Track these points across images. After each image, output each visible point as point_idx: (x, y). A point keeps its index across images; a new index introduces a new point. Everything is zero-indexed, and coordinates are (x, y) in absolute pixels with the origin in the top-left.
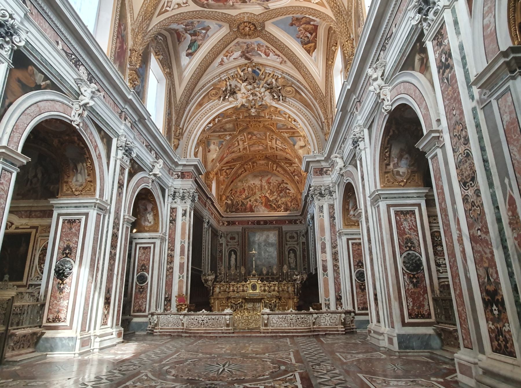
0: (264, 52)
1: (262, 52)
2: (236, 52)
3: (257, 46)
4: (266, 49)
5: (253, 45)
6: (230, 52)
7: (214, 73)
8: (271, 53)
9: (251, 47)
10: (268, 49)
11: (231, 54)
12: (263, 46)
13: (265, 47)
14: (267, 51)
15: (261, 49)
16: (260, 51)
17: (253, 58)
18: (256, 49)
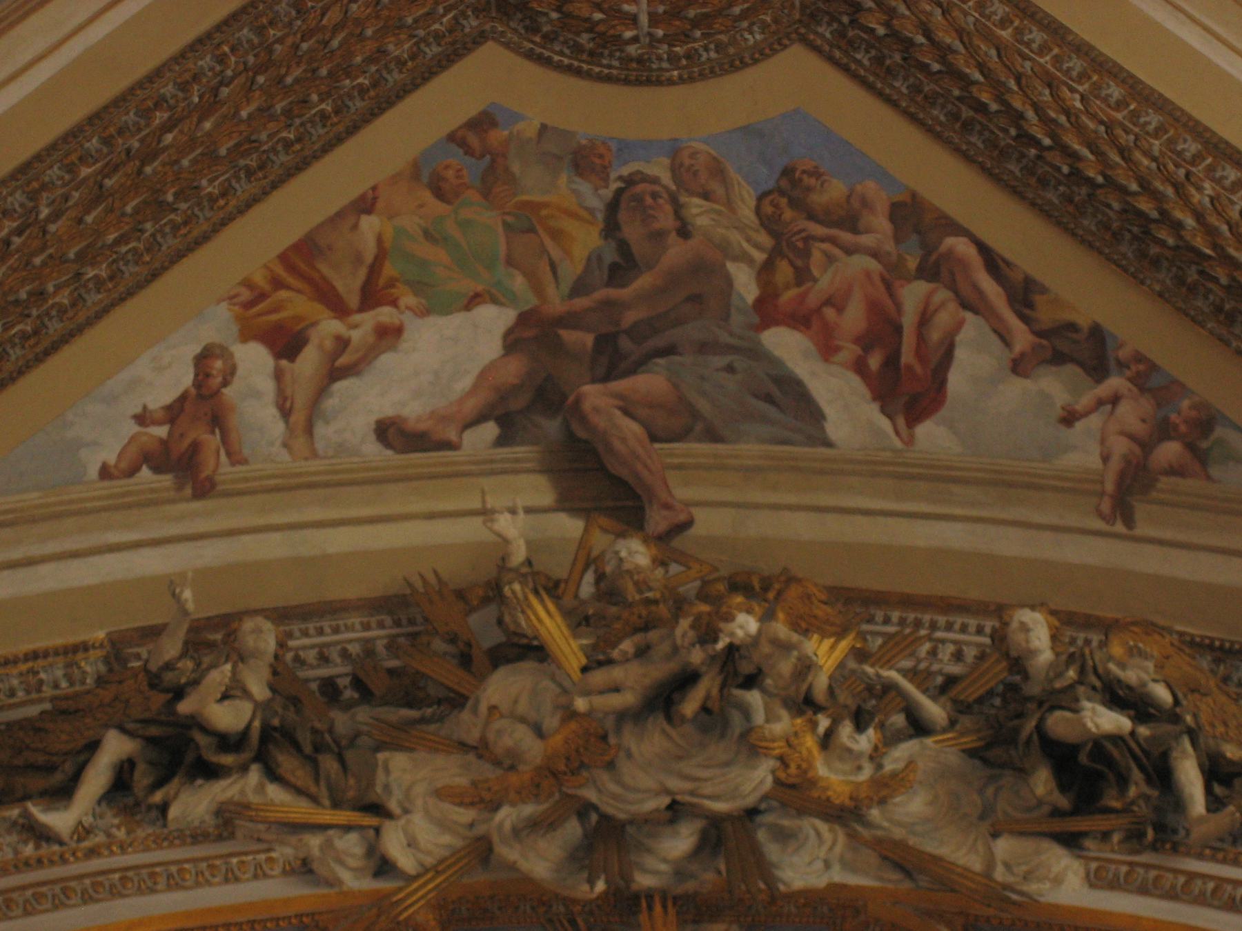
0: (866, 342)
1: (827, 350)
2: (433, 304)
3: (769, 223)
4: (893, 274)
5: (695, 207)
6: (348, 285)
7: (50, 578)
8: (973, 328)
9: (676, 253)
10: (931, 270)
11: (368, 321)
12: (850, 220)
13: (879, 229)
14: (913, 294)
15: (825, 282)
16: (800, 320)
17: (682, 493)
18: (746, 285)
